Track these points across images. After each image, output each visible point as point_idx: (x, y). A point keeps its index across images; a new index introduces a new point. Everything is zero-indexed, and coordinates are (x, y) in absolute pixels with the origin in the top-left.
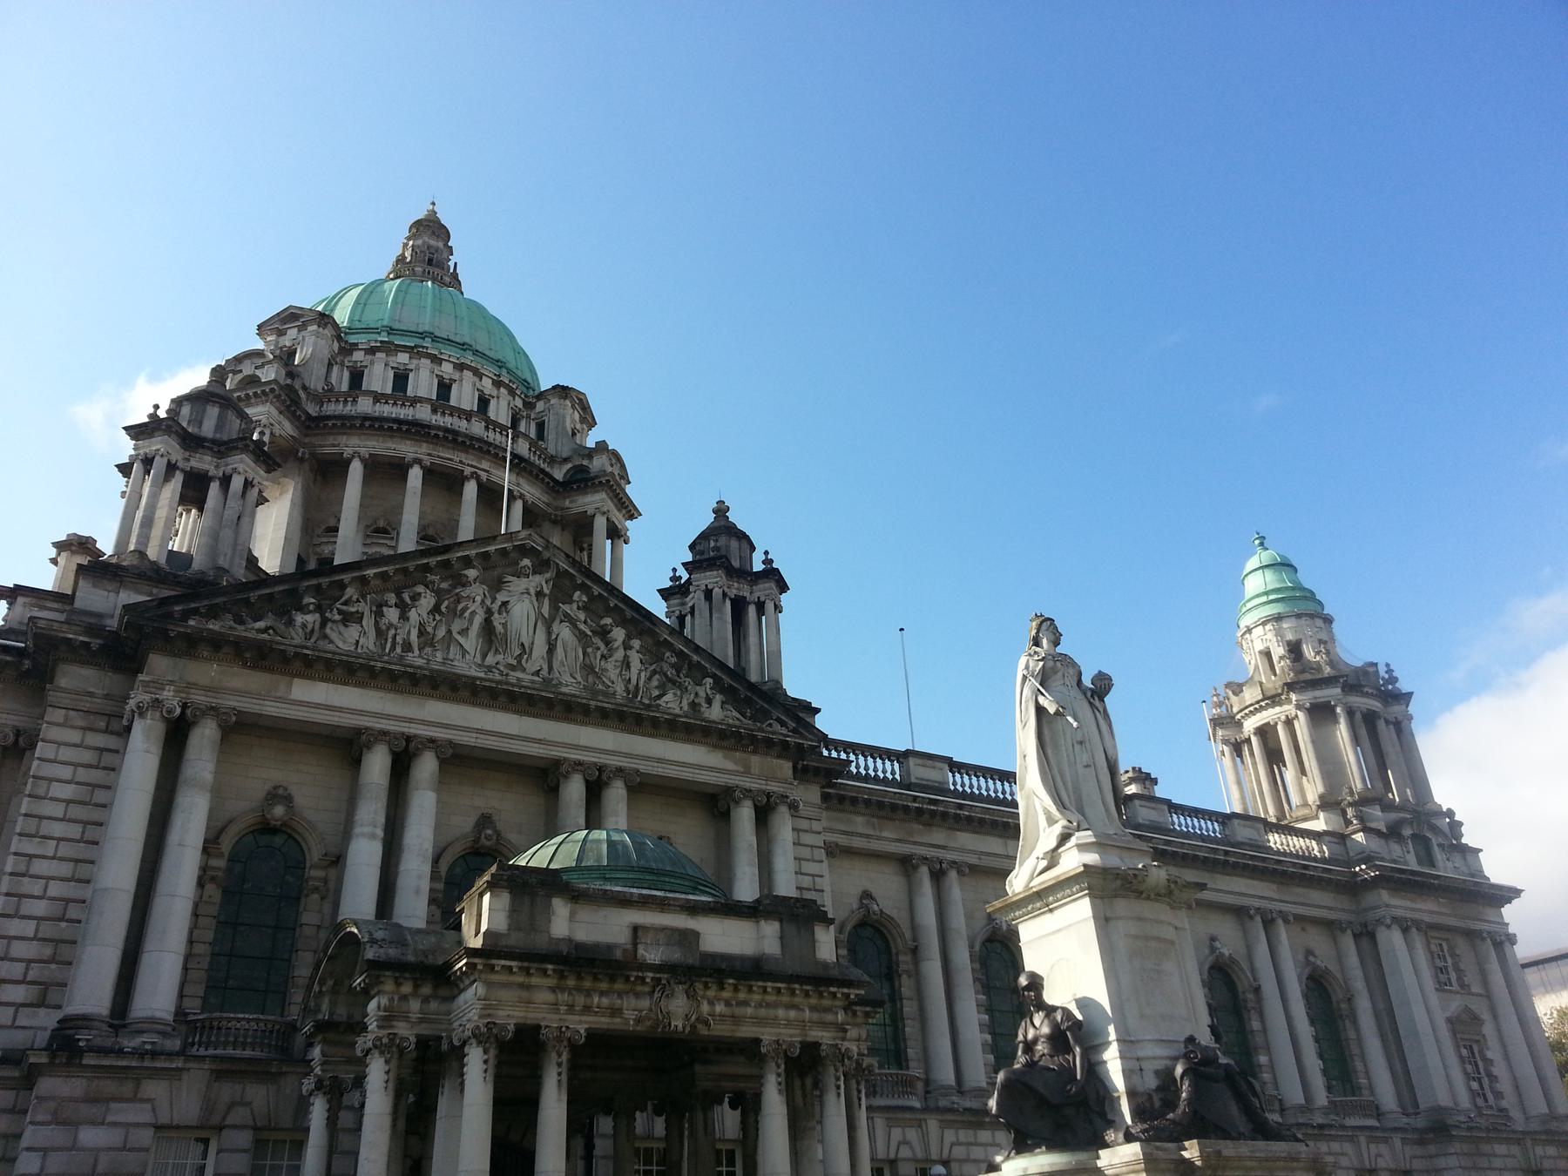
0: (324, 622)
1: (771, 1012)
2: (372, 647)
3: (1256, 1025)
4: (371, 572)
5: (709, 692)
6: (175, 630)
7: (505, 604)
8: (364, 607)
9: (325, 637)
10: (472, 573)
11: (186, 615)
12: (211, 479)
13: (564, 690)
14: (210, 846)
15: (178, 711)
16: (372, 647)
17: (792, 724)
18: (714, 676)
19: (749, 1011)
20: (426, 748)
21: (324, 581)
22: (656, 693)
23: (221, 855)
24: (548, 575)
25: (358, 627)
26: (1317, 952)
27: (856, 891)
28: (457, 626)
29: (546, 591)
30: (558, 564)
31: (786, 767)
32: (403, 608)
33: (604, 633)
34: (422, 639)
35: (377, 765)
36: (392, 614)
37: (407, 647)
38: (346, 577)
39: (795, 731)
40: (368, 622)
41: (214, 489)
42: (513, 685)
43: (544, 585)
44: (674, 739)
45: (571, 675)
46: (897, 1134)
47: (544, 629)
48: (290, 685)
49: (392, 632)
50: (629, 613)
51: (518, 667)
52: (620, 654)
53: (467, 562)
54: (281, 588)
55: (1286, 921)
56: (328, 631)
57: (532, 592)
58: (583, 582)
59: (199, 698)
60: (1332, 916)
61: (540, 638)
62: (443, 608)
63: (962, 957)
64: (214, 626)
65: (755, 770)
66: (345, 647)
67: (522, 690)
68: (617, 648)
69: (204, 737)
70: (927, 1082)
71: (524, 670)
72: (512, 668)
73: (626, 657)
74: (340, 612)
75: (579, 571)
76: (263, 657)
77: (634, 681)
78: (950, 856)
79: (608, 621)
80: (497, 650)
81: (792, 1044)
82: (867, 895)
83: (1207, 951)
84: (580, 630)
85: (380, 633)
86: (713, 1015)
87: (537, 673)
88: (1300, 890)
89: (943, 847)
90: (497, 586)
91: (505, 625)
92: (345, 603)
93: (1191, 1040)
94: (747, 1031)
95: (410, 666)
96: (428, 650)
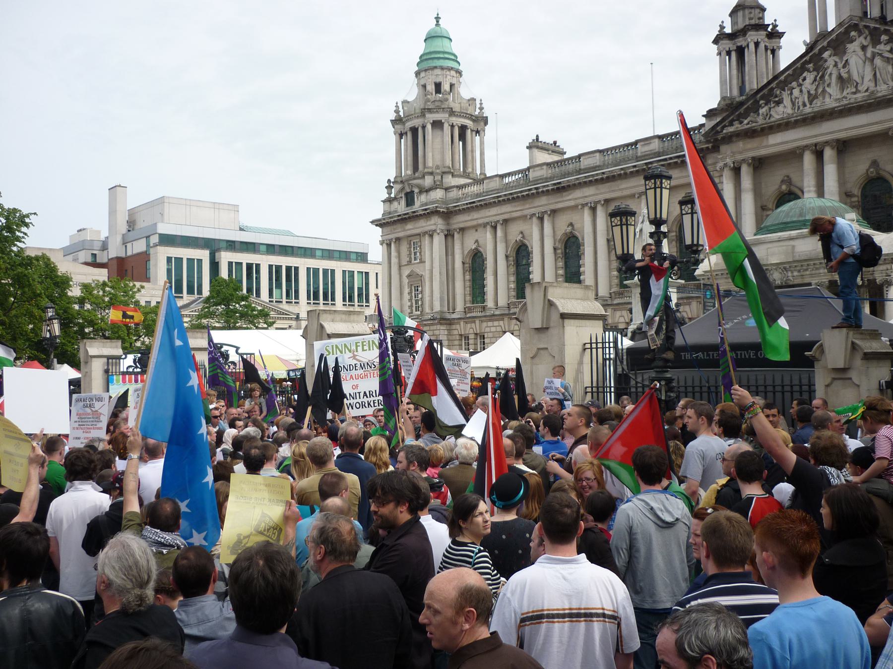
0: (770, 109)
1: (817, 272)
2: (790, 111)
6: (719, 137)
7: (847, 60)
9: (771, 116)
10: (826, 55)
11: (723, 128)
12: (744, 48)
13: (879, 95)
15: (732, 165)
19: (808, 273)
20: (824, 147)
21: (765, 91)
24: (865, 35)
25: (781, 105)
29: (865, 43)
30: (866, 27)
34: (811, 98)
35: (808, 159)
36: (796, 92)
38: (773, 85)
41: (746, 50)
42: (852, 104)
45: (884, 83)
47: (870, 64)
49: (797, 100)
54: (750, 103)
56: (772, 113)
57: (859, 50)
58: (885, 29)
59: (739, 157)
62: (818, 78)
64: (731, 129)
66: (778, 117)
67: (858, 104)
69: (745, 171)
71: (860, 91)
72: (855, 93)
74: (775, 102)
76: (751, 134)
80: (848, 87)
81: (825, 282)
84: (888, 58)
85: (793, 103)
87: (867, 90)
91: (848, 72)
92: (776, 97)
94: (807, 281)
95: (805, 114)
96: (815, 102)
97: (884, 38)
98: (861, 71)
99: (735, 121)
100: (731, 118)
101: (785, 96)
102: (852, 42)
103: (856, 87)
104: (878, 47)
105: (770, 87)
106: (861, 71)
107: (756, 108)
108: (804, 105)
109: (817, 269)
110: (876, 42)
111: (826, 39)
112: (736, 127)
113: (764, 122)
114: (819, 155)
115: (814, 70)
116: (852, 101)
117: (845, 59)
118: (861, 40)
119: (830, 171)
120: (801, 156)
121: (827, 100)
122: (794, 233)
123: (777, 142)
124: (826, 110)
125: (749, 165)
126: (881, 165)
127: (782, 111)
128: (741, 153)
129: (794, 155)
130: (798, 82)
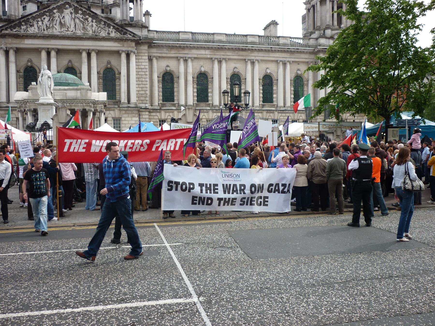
0: (27, 27)
1: (77, 105)
2: (37, 31)
3: (275, 88)
4: (34, 15)
5: (112, 30)
7: (64, 16)
8: (35, 23)
9: (27, 30)
10: (55, 11)
13: (78, 34)
14: (18, 71)
15: (5, 49)
16: (37, 31)
17: (132, 35)
18: (113, 26)
19: (73, 105)
21: (25, 19)
22: (99, 32)
23: (21, 72)
24: (72, 8)
25: (33, 28)
26: (301, 70)
27: (165, 65)
28: (54, 24)
31: (133, 44)
32: (42, 21)
33: (87, 19)
34: (47, 28)
35: (44, 54)
36: (40, 23)
37: (44, 30)
38: (30, 17)
39: (133, 36)
40: (36, 26)
43: (72, 10)
44: (105, 41)
46: (167, 114)
48: (24, 40)
49: (41, 27)
50: (92, 14)
51: (68, 31)
52: (91, 24)
53: (54, 8)
55: (290, 63)
57: (69, 13)
59: (9, 46)
60: (307, 60)
61: (73, 23)
63: (190, 78)
65: (125, 45)
68: (90, 23)
70: (178, 104)
71: (69, 31)
72: (67, 31)
73: (92, 24)
74: (30, 25)
75: (79, 6)
76: (17, 36)
77: (94, 30)
78: (189, 56)
79: (87, 17)
82: (168, 66)
83: (264, 71)
85: (38, 28)
86: (67, 105)
87: (72, 31)
88: (299, 55)
89: (187, 54)
90: (62, 12)
91: (64, 21)
92: (30, 23)
93: (46, 121)
96: (49, 30)
97: (80, 12)
98: (70, 23)
99: (8, 28)
100: (7, 26)
101: (35, 23)
102: (66, 9)
103: (68, 29)
104: (77, 15)
105: (28, 18)
106: (70, 23)
107: (20, 25)
108: (44, 30)
109: (77, 103)
110: (76, 12)
111: (56, 4)
112: (8, 31)
113: (24, 33)
114: (49, 54)
115: (49, 16)
116: (66, 34)
117: (63, 15)
118: (71, 9)
119: (54, 61)
120: (40, 52)
121: (54, 30)
122: (66, 88)
123: (29, 43)
124: (55, 35)
125: (14, 50)
126: (73, 62)
127: (33, 30)
128: (10, 44)
129: (38, 51)
130: (41, 19)
